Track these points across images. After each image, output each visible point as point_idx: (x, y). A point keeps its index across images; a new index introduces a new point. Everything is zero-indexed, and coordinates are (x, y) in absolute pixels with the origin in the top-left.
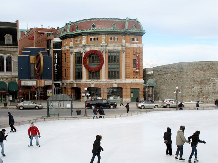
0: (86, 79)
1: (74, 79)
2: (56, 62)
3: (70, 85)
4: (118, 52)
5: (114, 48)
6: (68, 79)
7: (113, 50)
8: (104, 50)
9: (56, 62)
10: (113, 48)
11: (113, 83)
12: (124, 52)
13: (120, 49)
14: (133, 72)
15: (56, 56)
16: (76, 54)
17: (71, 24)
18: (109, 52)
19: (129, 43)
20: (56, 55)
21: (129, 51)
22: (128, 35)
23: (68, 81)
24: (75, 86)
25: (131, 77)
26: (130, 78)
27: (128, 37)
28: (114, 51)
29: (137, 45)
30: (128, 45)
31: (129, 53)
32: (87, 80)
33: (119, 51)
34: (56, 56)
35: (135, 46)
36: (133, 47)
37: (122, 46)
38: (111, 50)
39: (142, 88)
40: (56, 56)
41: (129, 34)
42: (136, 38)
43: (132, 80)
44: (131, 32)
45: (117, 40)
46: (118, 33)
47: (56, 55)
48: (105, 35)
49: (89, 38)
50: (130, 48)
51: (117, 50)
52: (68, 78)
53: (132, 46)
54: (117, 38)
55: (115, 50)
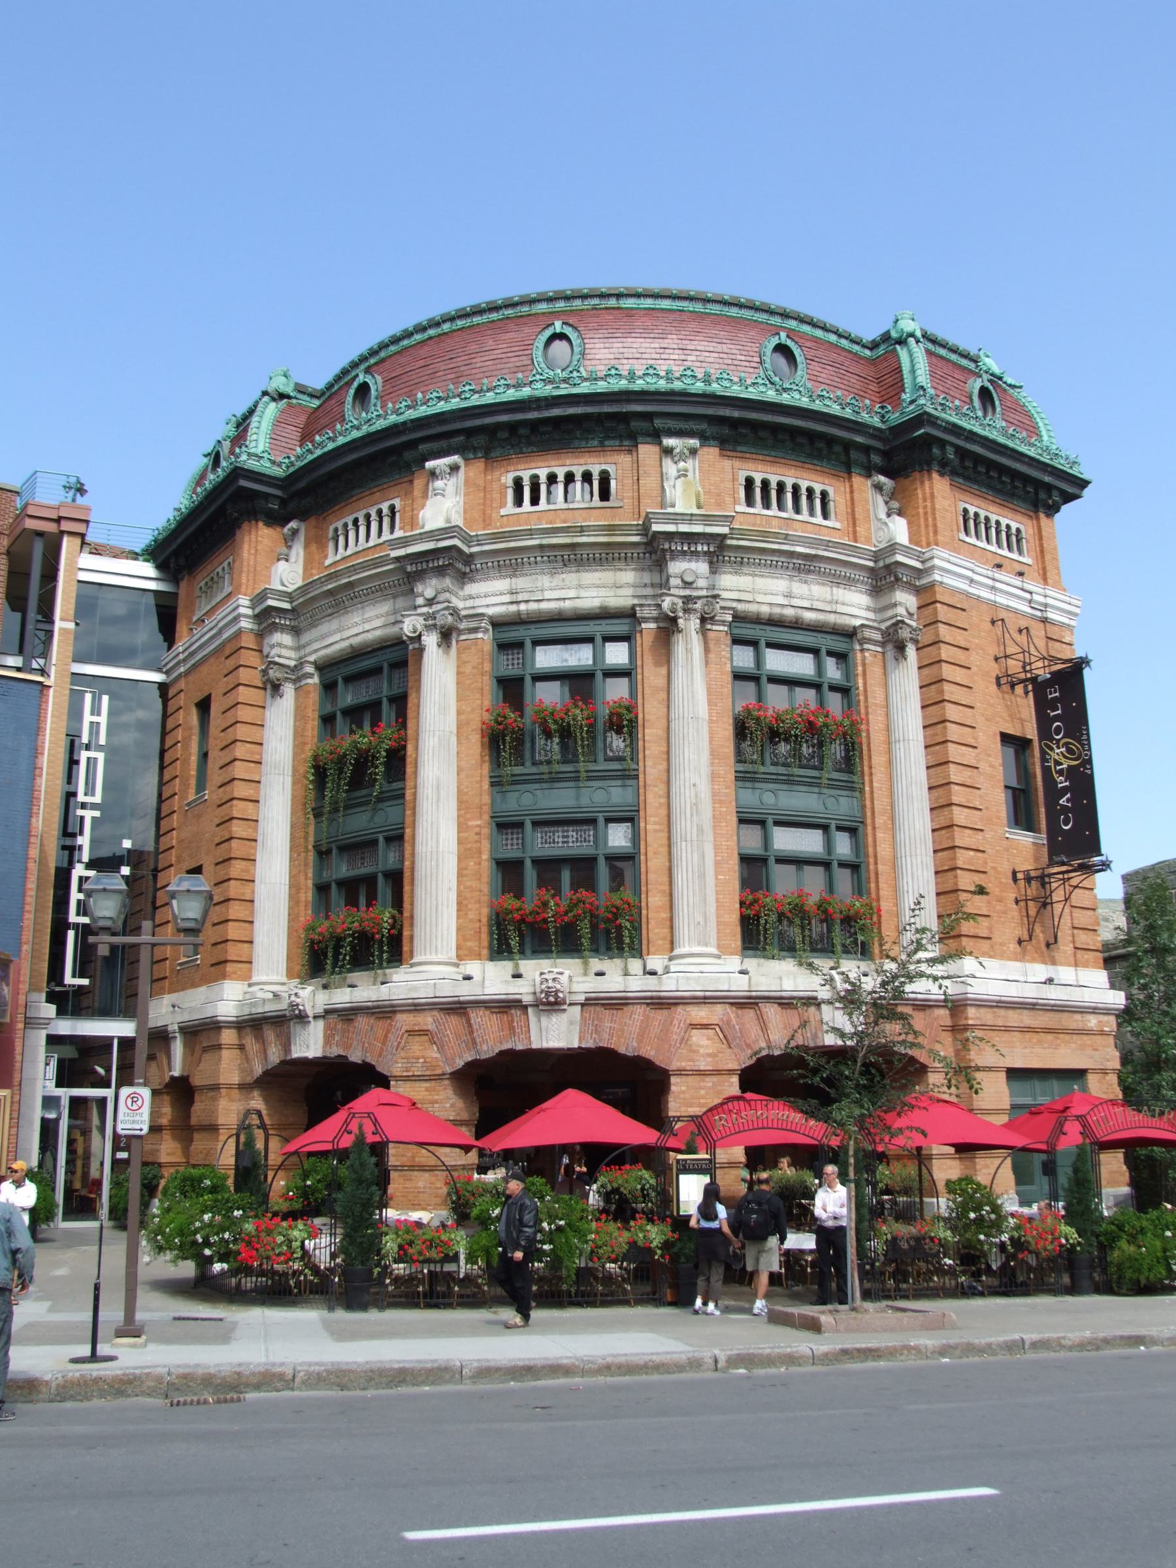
0: (463, 954)
1: (290, 974)
2: (90, 790)
3: (242, 1047)
4: (840, 641)
5: (799, 588)
6: (224, 976)
7: (789, 612)
8: (687, 599)
9: (90, 790)
10: (789, 596)
11: (812, 1001)
13: (853, 605)
14: (1014, 873)
15: (103, 720)
16: (329, 687)
17: (289, 390)
18: (751, 630)
19: (957, 547)
20: (96, 711)
22: (945, 468)
23: (228, 1000)
24: (310, 1044)
25: (997, 938)
26: (987, 945)
27: (941, 494)
28: (797, 625)
31: (960, 656)
32: (473, 967)
33: (850, 634)
34: (95, 726)
35: (1011, 595)
36: (994, 605)
38: (765, 610)
39: (1104, 1072)
40: (95, 726)
41: (951, 454)
43: (1014, 969)
44: (972, 436)
45: (825, 515)
46: (830, 440)
47: (96, 711)
48: (694, 442)
49: (508, 479)
51: (832, 618)
52: (220, 961)
53: (985, 594)
54: (824, 495)
55: (809, 616)
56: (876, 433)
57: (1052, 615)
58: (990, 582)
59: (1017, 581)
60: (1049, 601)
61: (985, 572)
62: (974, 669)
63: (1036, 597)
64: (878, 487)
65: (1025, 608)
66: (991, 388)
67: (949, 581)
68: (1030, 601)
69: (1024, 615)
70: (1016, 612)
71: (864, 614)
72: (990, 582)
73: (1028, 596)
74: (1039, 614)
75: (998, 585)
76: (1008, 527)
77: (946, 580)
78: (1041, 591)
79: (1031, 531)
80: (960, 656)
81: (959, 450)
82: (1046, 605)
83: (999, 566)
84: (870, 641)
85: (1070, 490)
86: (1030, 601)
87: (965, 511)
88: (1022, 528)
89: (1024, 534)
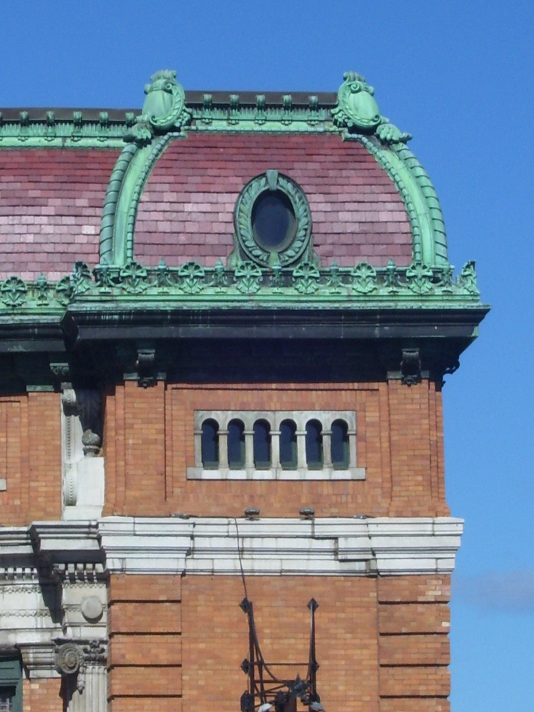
12: (93, 680)
21: (160, 650)
29: (326, 525)
30: (147, 546)
31: (159, 680)
36: (243, 577)
37: (50, 574)
42: (301, 419)
44: (181, 317)
50: (179, 591)
53: (226, 564)
56: (45, 331)
57: (383, 564)
58: (233, 544)
59: (304, 527)
60: (375, 543)
61: (222, 530)
62: (186, 692)
63: (342, 544)
64: (69, 409)
65: (330, 565)
66: (288, 187)
67: (138, 563)
68: (336, 552)
69: (324, 577)
70: (306, 577)
71: (31, 622)
72: (233, 544)
73: (328, 544)
74: (362, 566)
75: (247, 544)
76: (314, 426)
77: (130, 564)
78: (359, 529)
79: (372, 416)
80: (159, 680)
81: (158, 343)
82: (373, 552)
83: (252, 515)
84: (38, 665)
85: (455, 331)
86: (336, 552)
87: (211, 425)
88: (348, 417)
89: (352, 428)
